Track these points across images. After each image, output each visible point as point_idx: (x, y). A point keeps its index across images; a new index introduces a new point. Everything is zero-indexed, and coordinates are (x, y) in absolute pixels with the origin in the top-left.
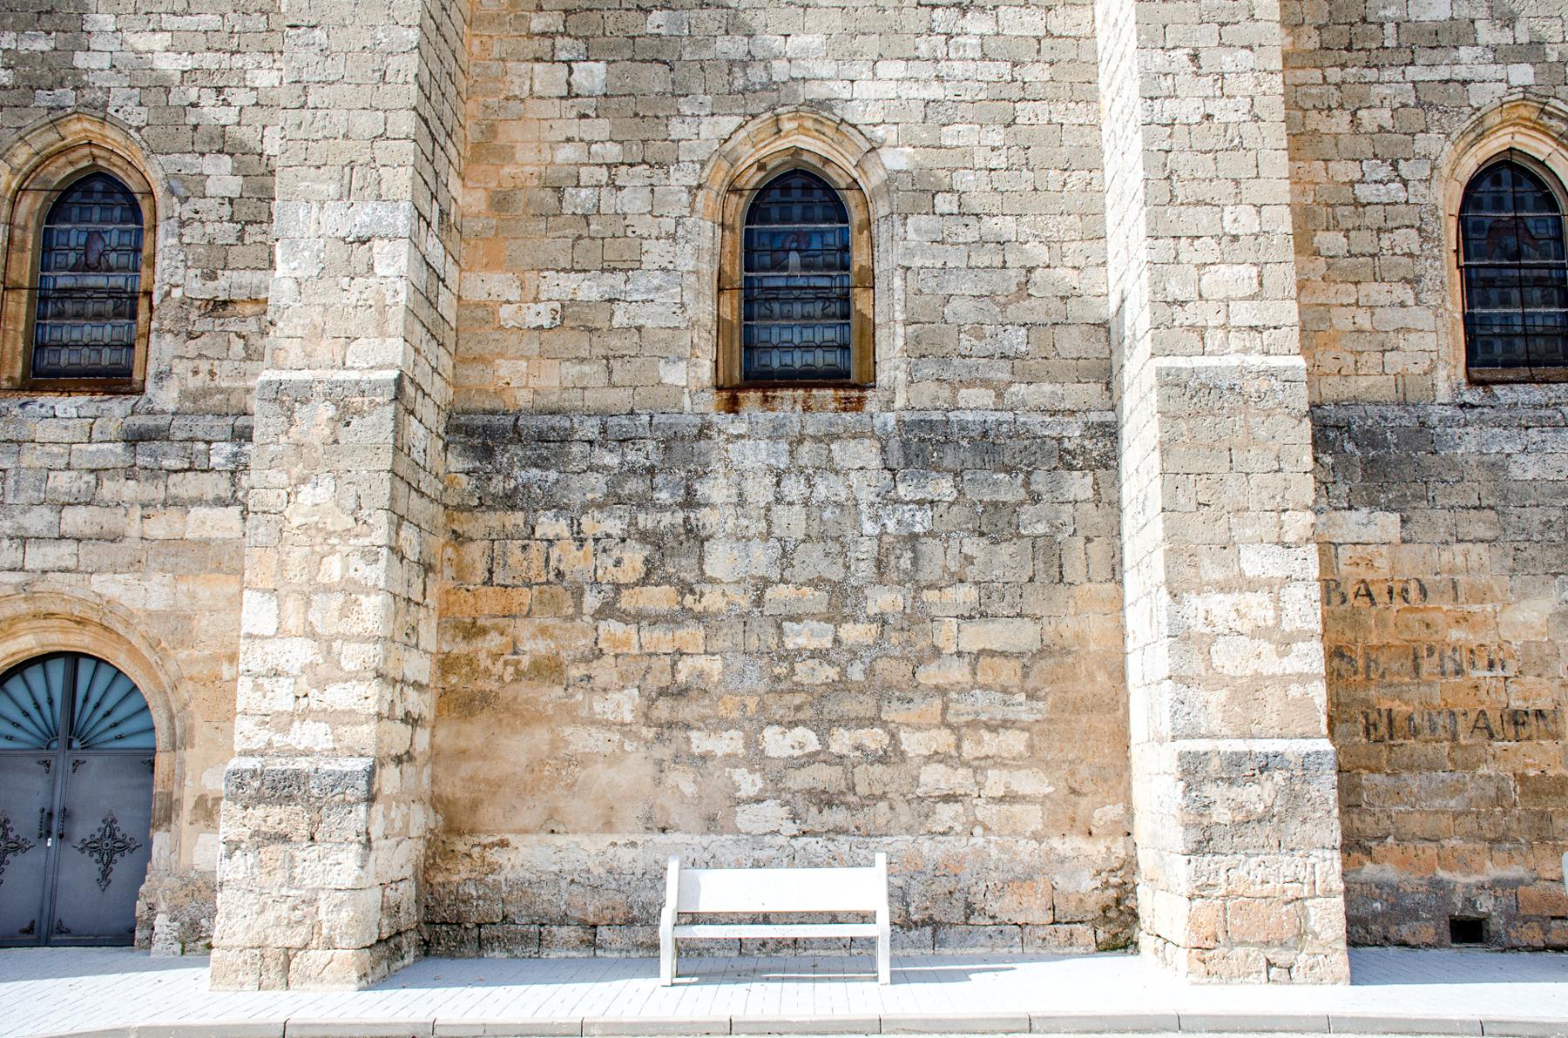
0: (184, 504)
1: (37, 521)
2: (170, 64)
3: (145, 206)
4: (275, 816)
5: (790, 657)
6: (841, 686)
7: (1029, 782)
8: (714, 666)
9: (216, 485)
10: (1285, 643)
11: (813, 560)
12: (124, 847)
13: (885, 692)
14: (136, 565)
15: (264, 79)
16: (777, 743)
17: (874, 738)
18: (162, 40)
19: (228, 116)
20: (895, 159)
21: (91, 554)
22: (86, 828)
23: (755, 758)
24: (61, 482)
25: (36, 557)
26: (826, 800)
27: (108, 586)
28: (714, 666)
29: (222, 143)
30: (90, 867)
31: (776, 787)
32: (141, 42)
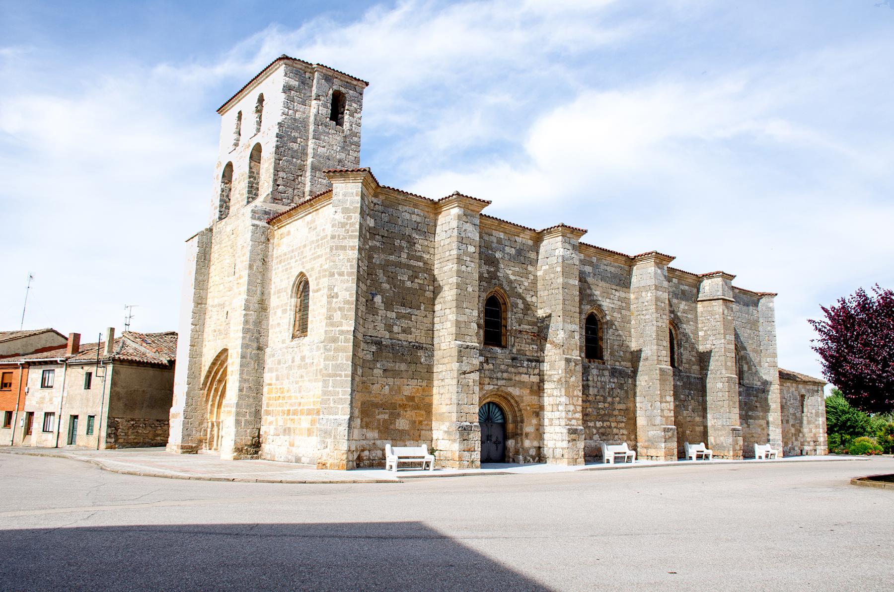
0: (521, 373)
1: (499, 375)
2: (512, 277)
3: (503, 307)
4: (573, 436)
5: (599, 409)
6: (605, 414)
7: (625, 432)
8: (590, 410)
9: (524, 370)
10: (670, 411)
11: (602, 392)
12: (500, 443)
13: (610, 415)
14: (514, 386)
15: (526, 284)
16: (599, 424)
17: (608, 423)
18: (510, 272)
19: (521, 291)
20: (608, 318)
21: (508, 383)
22: (494, 439)
23: (595, 427)
24: (502, 367)
25: (500, 383)
26: (603, 434)
27: (510, 389)
28: (590, 410)
29: (520, 296)
30: (494, 445)
31: (598, 433)
32: (510, 272)
